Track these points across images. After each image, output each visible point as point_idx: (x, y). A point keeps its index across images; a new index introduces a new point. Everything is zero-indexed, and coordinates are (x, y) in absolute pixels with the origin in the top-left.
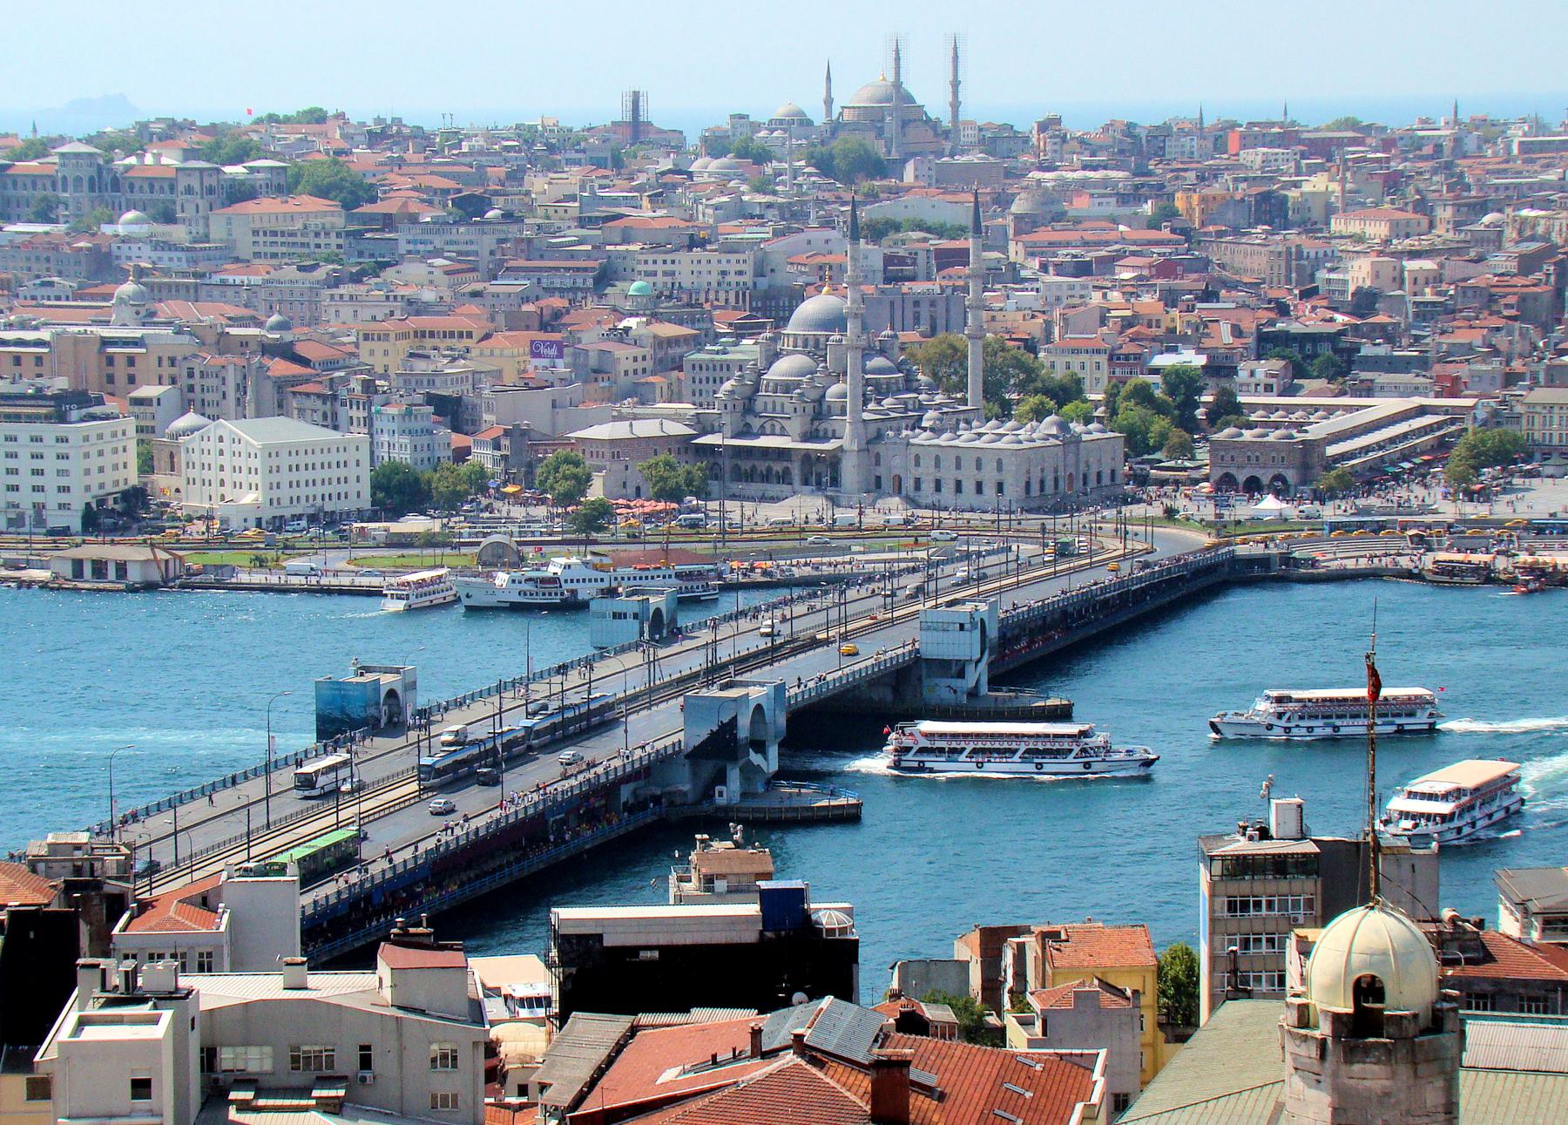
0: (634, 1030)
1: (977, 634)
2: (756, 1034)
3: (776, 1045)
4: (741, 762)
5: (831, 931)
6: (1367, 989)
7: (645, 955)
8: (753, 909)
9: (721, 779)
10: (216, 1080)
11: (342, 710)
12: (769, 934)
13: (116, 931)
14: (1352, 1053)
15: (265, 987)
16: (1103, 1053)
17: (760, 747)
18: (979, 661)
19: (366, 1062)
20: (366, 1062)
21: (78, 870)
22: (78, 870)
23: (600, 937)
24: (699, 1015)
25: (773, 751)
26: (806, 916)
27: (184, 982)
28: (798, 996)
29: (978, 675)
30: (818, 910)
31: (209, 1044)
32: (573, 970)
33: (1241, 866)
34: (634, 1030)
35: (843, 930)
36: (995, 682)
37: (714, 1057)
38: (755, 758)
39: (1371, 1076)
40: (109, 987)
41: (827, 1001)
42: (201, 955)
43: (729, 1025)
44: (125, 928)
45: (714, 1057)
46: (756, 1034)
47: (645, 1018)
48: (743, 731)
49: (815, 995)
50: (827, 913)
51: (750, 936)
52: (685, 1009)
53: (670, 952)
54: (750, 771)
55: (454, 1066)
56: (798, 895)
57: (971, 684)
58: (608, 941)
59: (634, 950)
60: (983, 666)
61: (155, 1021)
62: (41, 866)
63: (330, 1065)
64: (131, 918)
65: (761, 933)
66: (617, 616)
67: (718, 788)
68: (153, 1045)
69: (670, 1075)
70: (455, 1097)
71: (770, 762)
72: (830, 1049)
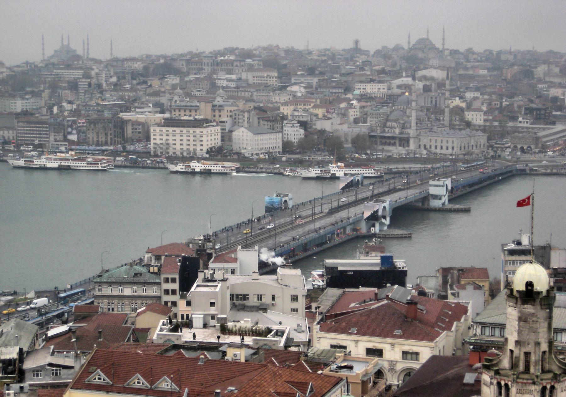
0: (344, 292)
1: (445, 188)
4: (379, 221)
5: (400, 268)
6: (529, 284)
7: (350, 273)
8: (378, 260)
9: (374, 226)
10: (234, 303)
11: (272, 205)
12: (383, 268)
14: (524, 302)
16: (471, 302)
17: (384, 217)
18: (445, 195)
19: (273, 299)
21: (200, 246)
22: (200, 246)
23: (337, 268)
24: (362, 289)
25: (388, 219)
26: (393, 264)
29: (445, 199)
30: (396, 262)
31: (233, 293)
32: (330, 276)
33: (512, 252)
35: (403, 268)
36: (450, 201)
37: (365, 300)
38: (383, 220)
39: (529, 309)
41: (396, 286)
42: (232, 270)
43: (370, 292)
45: (365, 300)
47: (347, 290)
48: (380, 213)
49: (393, 284)
50: (399, 263)
51: (378, 269)
52: (358, 288)
53: (355, 272)
54: (382, 224)
55: (297, 301)
56: (391, 257)
57: (443, 201)
58: (340, 268)
59: (346, 271)
60: (446, 196)
65: (381, 268)
67: (372, 228)
69: (352, 305)
70: (297, 309)
71: (387, 222)
72: (396, 299)
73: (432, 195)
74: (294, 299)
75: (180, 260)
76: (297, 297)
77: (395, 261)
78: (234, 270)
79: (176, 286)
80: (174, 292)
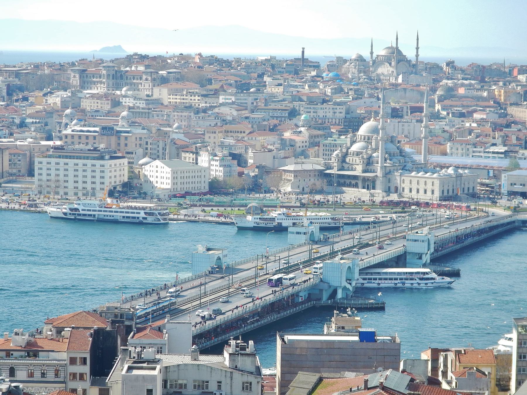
0: (320, 380)
2: (366, 382)
3: (372, 386)
13: (129, 338)
15: (187, 360)
19: (219, 387)
20: (219, 387)
21: (116, 316)
27: (158, 356)
28: (380, 369)
34: (320, 380)
37: (351, 389)
40: (132, 357)
44: (133, 337)
46: (366, 382)
49: (386, 369)
55: (251, 390)
60: (428, 256)
61: (154, 369)
62: (104, 314)
63: (207, 388)
64: (134, 334)
66: (298, 233)
68: (154, 377)
72: (392, 388)
73: (410, 253)
74: (247, 387)
75: (91, 334)
76: (251, 383)
77: (378, 338)
78: (161, 348)
79: (86, 369)
80: (82, 377)
